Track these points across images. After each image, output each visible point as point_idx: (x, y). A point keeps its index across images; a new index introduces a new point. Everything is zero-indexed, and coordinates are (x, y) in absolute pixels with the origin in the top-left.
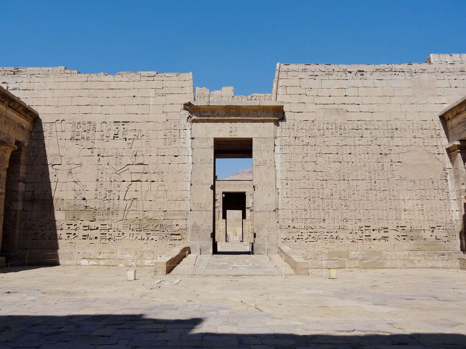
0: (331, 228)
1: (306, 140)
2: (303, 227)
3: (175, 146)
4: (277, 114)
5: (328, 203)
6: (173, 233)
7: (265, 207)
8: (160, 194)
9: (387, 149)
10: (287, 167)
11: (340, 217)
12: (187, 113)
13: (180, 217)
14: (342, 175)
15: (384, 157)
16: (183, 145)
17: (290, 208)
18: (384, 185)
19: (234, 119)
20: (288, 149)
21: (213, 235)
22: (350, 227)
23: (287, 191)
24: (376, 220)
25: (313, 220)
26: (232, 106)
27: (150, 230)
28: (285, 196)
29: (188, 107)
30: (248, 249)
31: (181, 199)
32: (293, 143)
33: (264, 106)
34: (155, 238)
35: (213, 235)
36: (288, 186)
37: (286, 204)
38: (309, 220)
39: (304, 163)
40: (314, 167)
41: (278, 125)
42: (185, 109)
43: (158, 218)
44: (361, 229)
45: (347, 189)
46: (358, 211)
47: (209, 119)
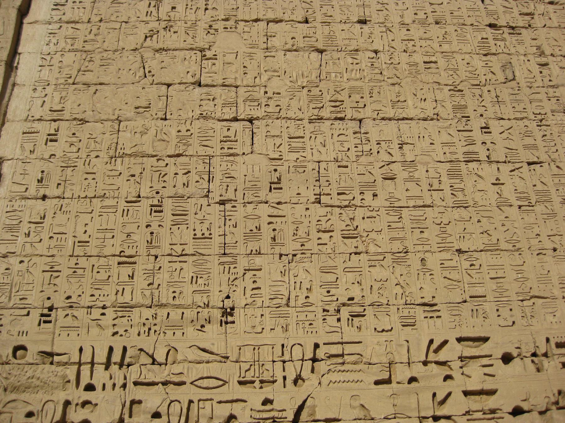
0: (266, 355)
2: (101, 357)
5: (251, 225)
9: (516, 12)
11: (318, 295)
14: (327, 97)
15: (506, 35)
17: (41, 249)
18: (529, 141)
22: (373, 346)
23: (46, 166)
24: (515, 305)
25: (164, 312)
28: (32, 191)
39: (148, 54)
40: (195, 68)
44: (442, 356)
45: (352, 154)
46: (414, 260)
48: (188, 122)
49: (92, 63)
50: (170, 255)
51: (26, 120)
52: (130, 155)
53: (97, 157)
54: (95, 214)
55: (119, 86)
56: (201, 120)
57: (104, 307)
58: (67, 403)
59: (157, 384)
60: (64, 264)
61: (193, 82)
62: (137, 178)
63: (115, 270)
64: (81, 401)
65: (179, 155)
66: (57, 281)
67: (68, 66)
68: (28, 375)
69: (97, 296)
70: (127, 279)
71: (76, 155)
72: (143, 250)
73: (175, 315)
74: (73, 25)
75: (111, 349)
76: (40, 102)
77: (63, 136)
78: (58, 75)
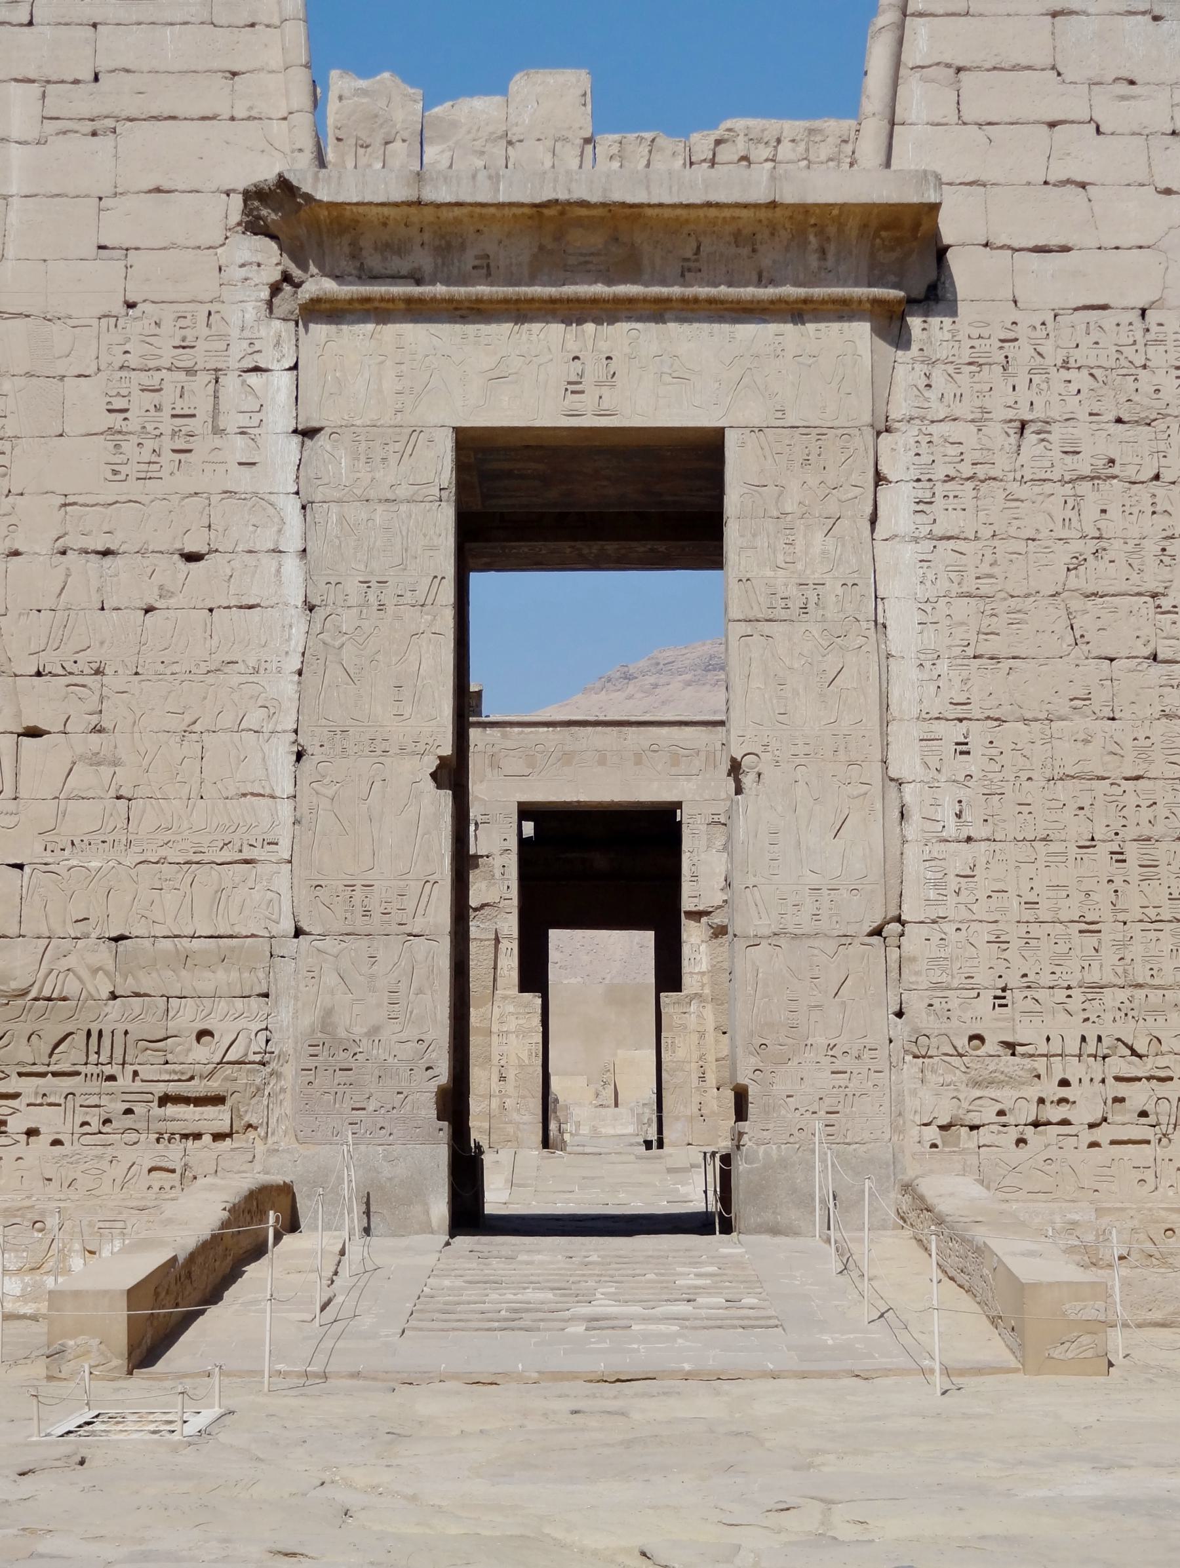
1: (1097, 445)
2: (1073, 1046)
3: (184, 482)
4: (898, 265)
6: (172, 1089)
7: (809, 907)
8: (84, 818)
10: (959, 632)
12: (267, 258)
13: (221, 978)
16: (244, 480)
17: (980, 910)
19: (595, 301)
20: (969, 503)
21: (454, 1104)
23: (963, 793)
25: (1140, 994)
26: (583, 204)
27: (12, 1071)
28: (951, 831)
29: (276, 209)
30: (696, 1195)
31: (226, 855)
32: (1002, 464)
33: (805, 209)
34: (49, 1121)
35: (454, 1104)
36: (973, 765)
37: (953, 883)
38: (1113, 998)
39: (1076, 604)
40: (1147, 631)
41: (899, 338)
42: (254, 226)
43: (71, 987)
47: (421, 301)
48: (1147, 723)
49: (995, 619)
50: (1141, 921)
51: (918, 718)
52: (1073, 777)
53: (1029, 779)
54: (1041, 864)
55: (1042, 661)
56: (1164, 720)
57: (1069, 987)
58: (1041, 1101)
59: (1139, 1079)
60: (1014, 934)
61: (1146, 655)
62: (1086, 811)
63: (1077, 938)
64: (1056, 1099)
65: (1137, 778)
66: (1005, 955)
67: (962, 624)
68: (991, 1068)
69: (1059, 974)
70: (1093, 952)
71: (1000, 776)
72: (1107, 914)
73: (1155, 997)
74: (951, 544)
75: (1083, 1039)
76: (933, 689)
77: (976, 744)
78: (948, 641)
